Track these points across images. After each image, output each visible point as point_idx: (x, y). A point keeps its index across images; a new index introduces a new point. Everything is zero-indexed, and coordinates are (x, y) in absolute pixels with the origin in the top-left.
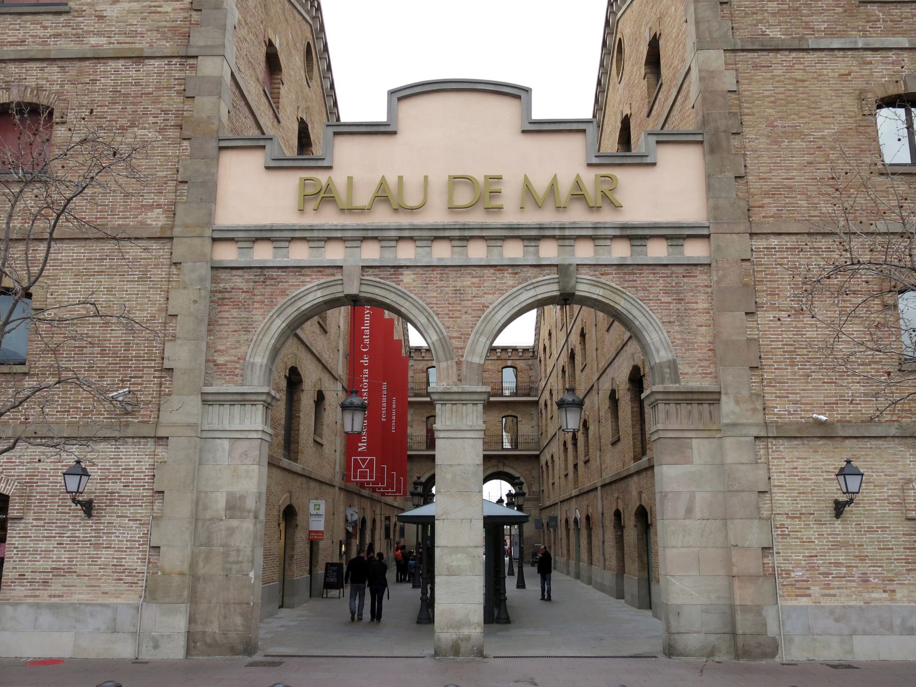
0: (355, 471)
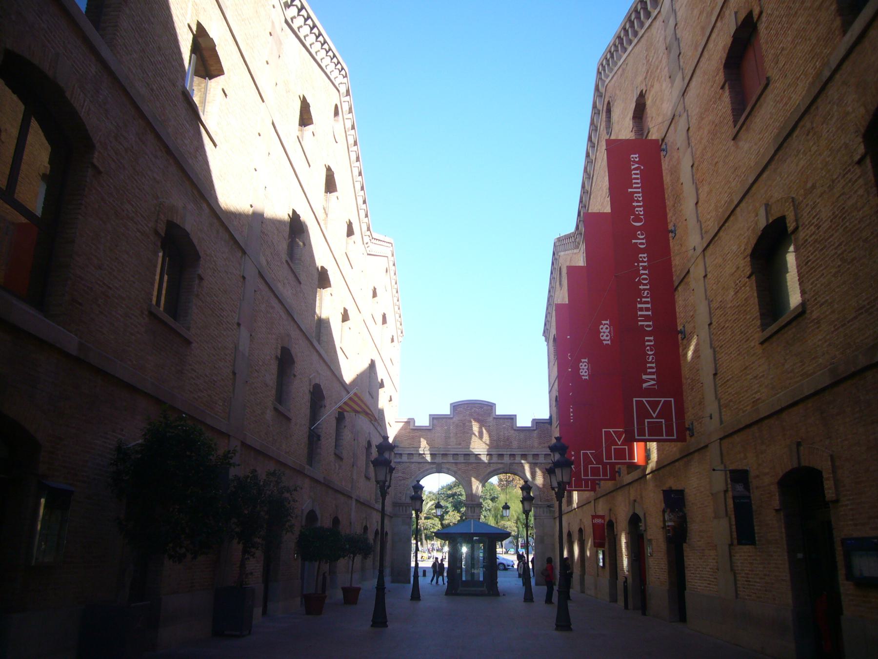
0: (641, 423)
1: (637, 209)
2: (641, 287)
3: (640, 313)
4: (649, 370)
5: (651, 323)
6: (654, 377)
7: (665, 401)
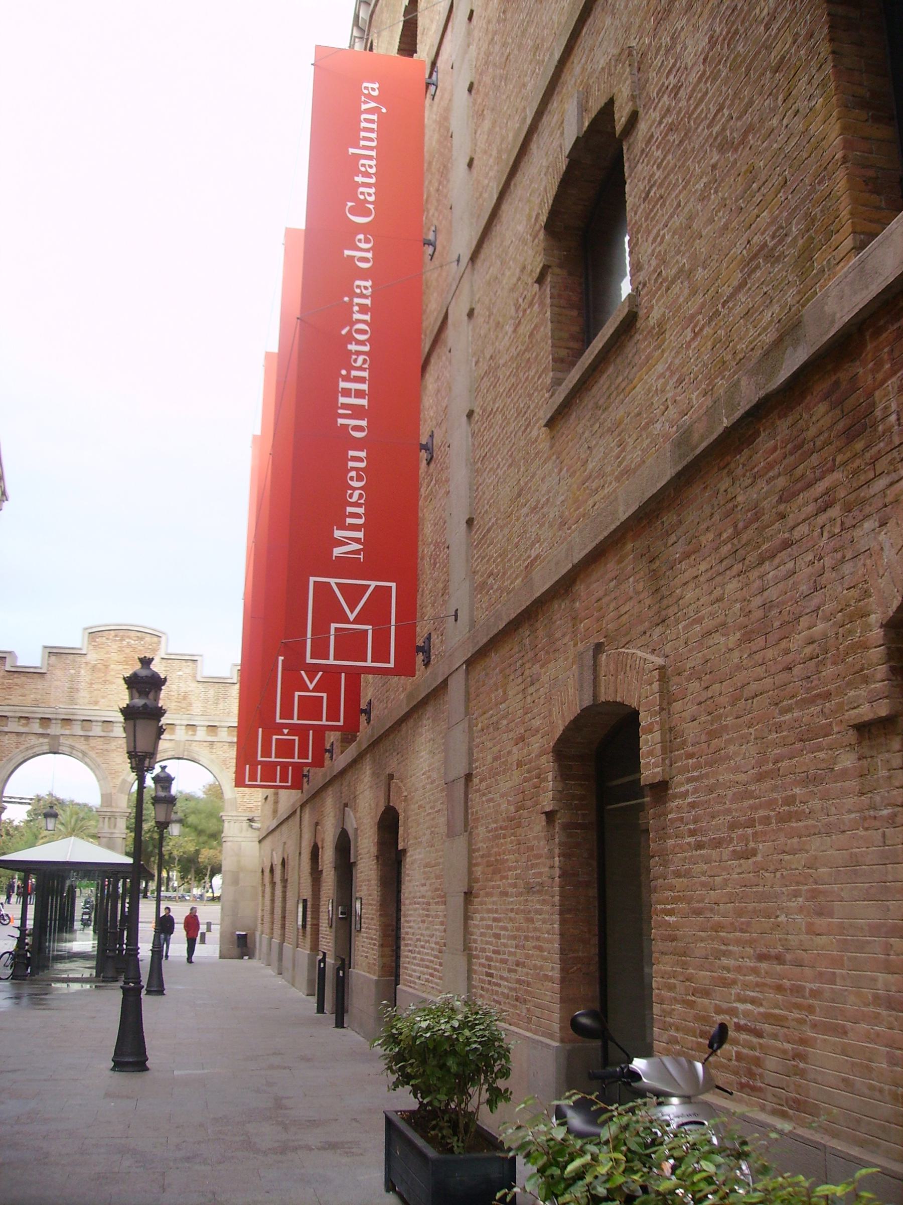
0: (321, 628)
1: (361, 189)
2: (352, 347)
3: (342, 400)
4: (349, 521)
5: (364, 423)
6: (360, 535)
7: (376, 586)
